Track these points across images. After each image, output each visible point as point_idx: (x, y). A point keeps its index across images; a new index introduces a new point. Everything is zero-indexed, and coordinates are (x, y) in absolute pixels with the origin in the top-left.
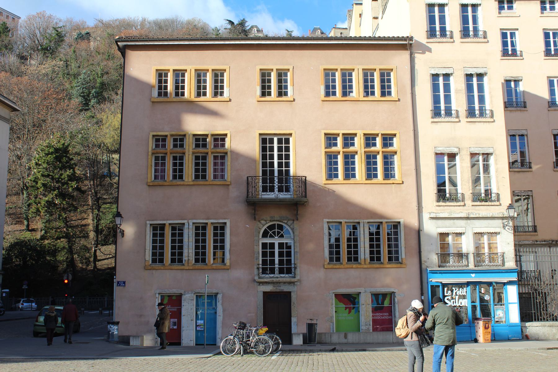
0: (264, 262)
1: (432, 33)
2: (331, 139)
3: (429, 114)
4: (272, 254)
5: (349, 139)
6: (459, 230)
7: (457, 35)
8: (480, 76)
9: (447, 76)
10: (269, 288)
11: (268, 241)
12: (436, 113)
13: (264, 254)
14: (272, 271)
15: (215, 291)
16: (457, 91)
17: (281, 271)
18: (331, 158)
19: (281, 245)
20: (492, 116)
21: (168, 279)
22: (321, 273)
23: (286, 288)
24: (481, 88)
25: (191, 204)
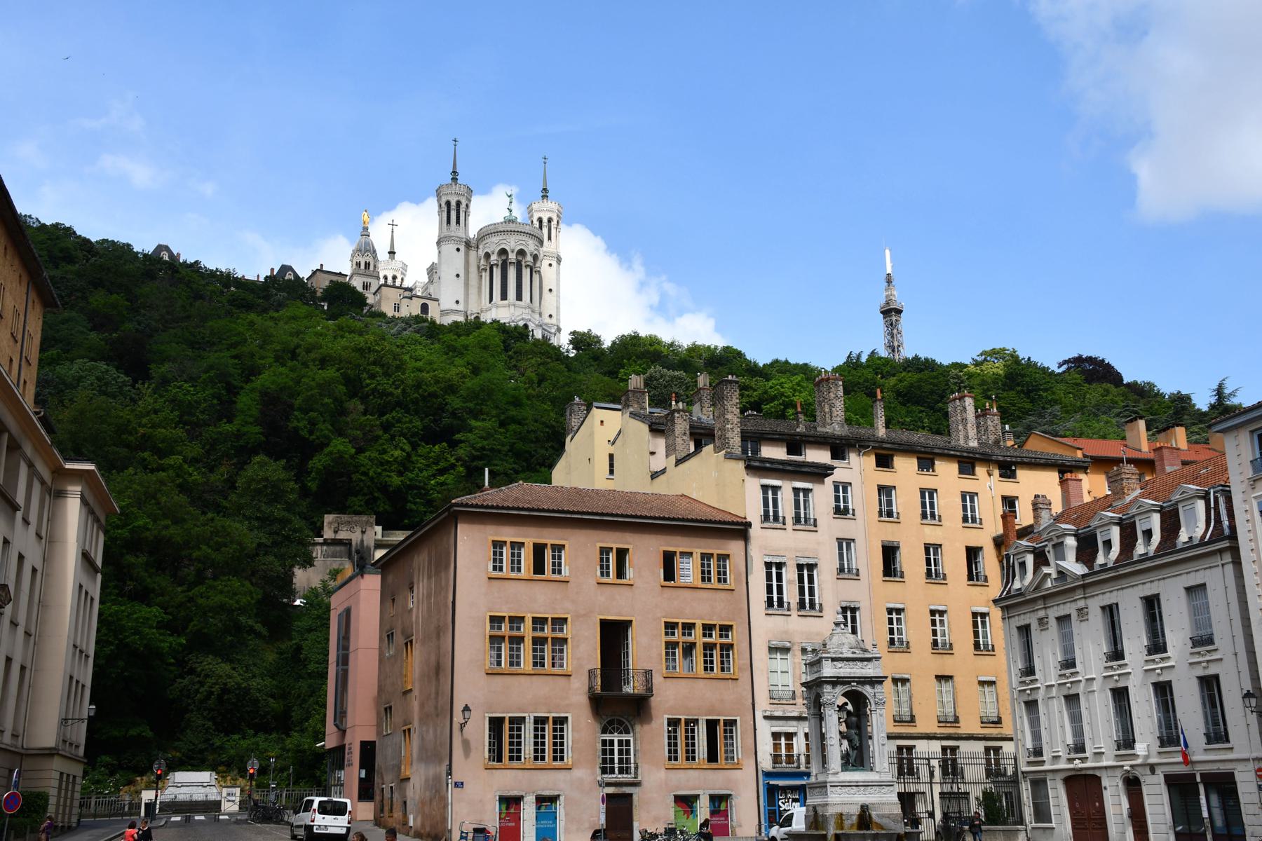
0: (604, 761)
1: (766, 517)
2: (670, 627)
3: (763, 605)
4: (612, 752)
5: (689, 627)
6: (791, 730)
7: (789, 521)
8: (811, 567)
9: (780, 566)
10: (611, 790)
11: (607, 737)
12: (770, 603)
13: (604, 752)
14: (612, 772)
15: (556, 793)
16: (789, 582)
17: (621, 772)
18: (671, 646)
19: (620, 742)
20: (821, 611)
21: (509, 780)
22: (662, 774)
23: (627, 790)
24: (811, 580)
25: (528, 696)
